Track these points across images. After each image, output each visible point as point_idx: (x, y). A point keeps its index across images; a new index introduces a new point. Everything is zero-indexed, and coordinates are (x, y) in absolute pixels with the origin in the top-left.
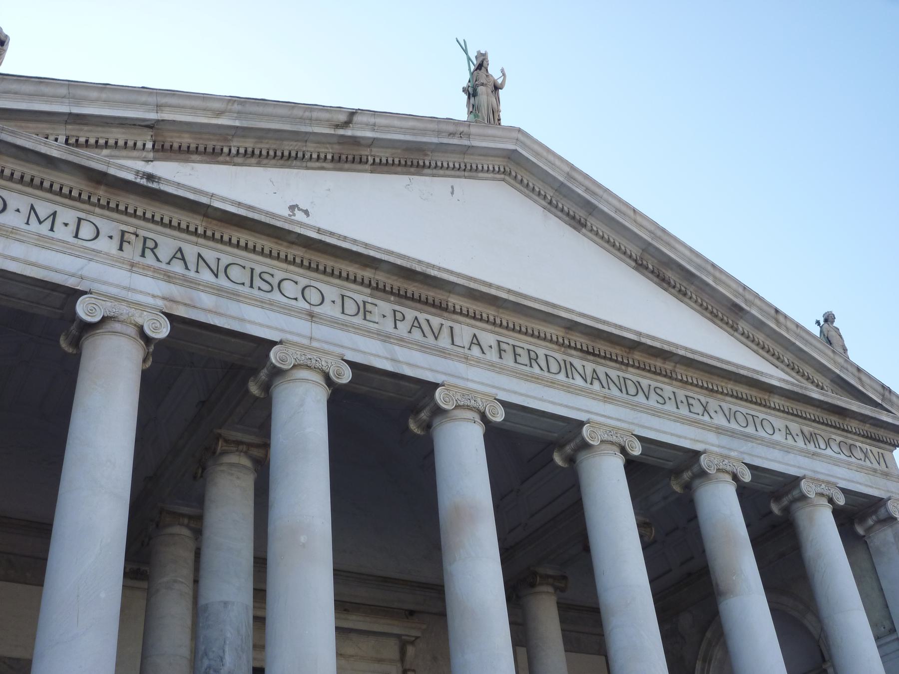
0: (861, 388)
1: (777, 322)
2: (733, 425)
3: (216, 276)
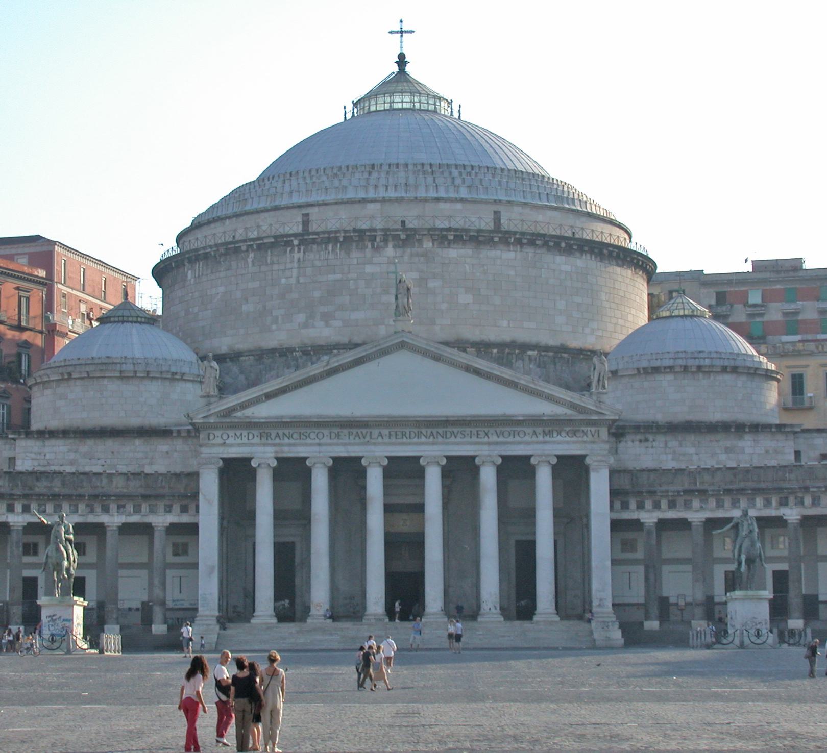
0: (583, 404)
1: (535, 384)
2: (501, 439)
3: (289, 439)
